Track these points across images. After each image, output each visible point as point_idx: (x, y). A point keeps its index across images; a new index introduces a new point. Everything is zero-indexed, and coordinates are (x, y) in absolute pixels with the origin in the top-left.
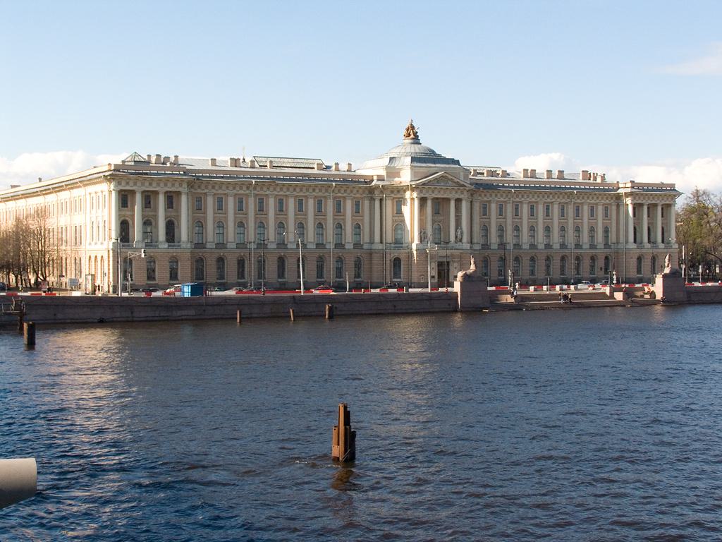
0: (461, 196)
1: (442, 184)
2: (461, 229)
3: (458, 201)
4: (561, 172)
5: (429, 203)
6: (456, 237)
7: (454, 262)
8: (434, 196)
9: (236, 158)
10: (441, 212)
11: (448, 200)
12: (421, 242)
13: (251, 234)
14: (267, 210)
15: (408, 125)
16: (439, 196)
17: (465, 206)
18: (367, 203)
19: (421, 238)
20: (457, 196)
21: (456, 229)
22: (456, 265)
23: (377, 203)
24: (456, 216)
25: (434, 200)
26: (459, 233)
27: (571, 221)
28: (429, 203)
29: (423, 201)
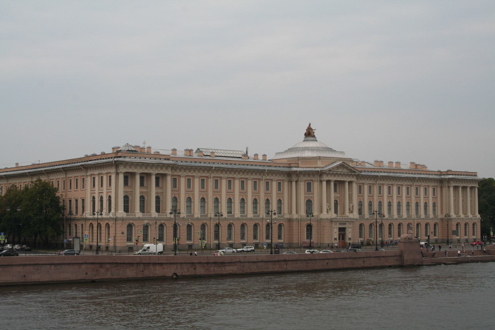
1: (340, 170)
3: (350, 183)
9: (190, 149)
12: (327, 212)
18: (286, 184)
22: (350, 230)
23: (294, 184)
28: (332, 184)
29: (328, 182)
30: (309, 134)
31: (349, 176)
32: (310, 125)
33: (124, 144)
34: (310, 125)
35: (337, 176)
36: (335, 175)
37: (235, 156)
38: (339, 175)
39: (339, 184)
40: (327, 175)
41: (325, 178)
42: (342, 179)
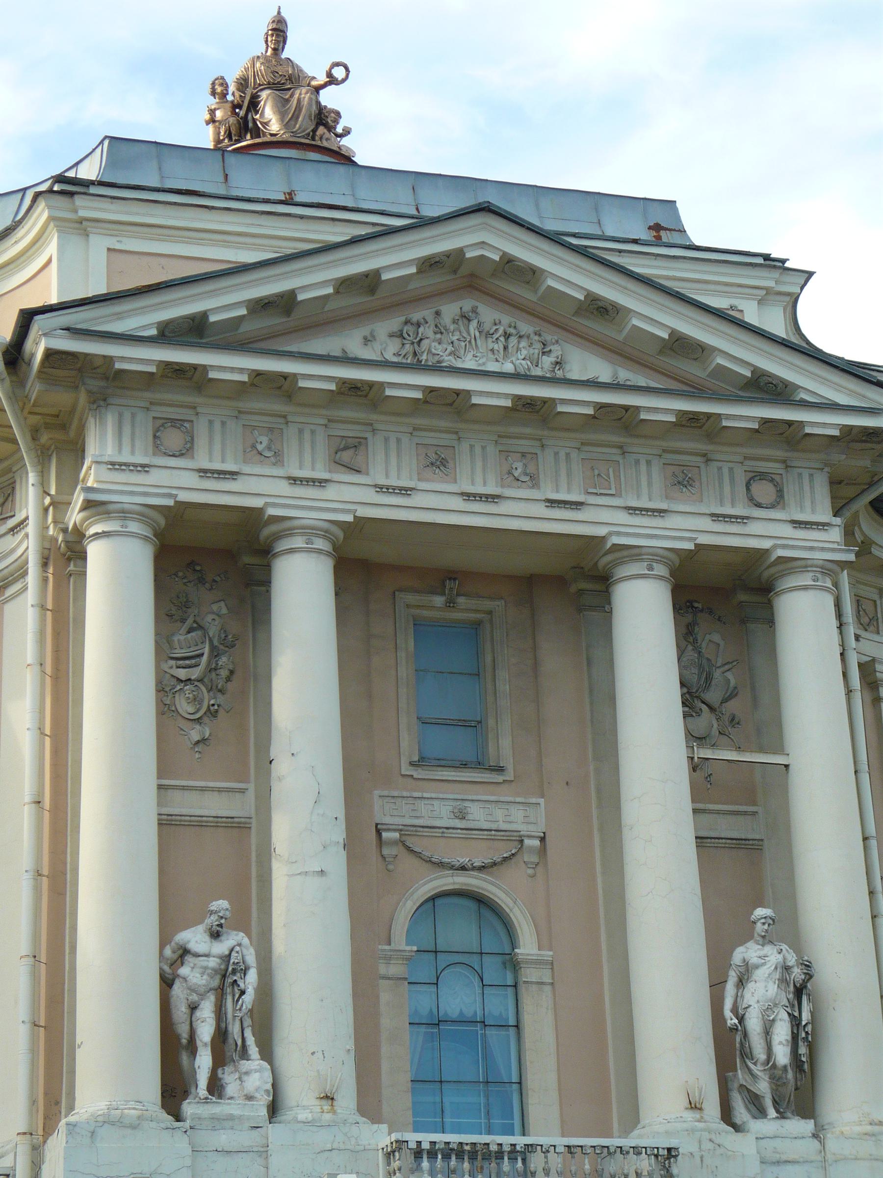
0: (765, 532)
2: (787, 929)
3: (725, 602)
5: (302, 593)
6: (730, 1046)
8: (351, 497)
10: (504, 746)
11: (578, 582)
12: (174, 1092)
15: (238, 53)
19: (174, 1047)
20: (690, 525)
21: (723, 935)
24: (707, 784)
25: (364, 566)
26: (762, 992)
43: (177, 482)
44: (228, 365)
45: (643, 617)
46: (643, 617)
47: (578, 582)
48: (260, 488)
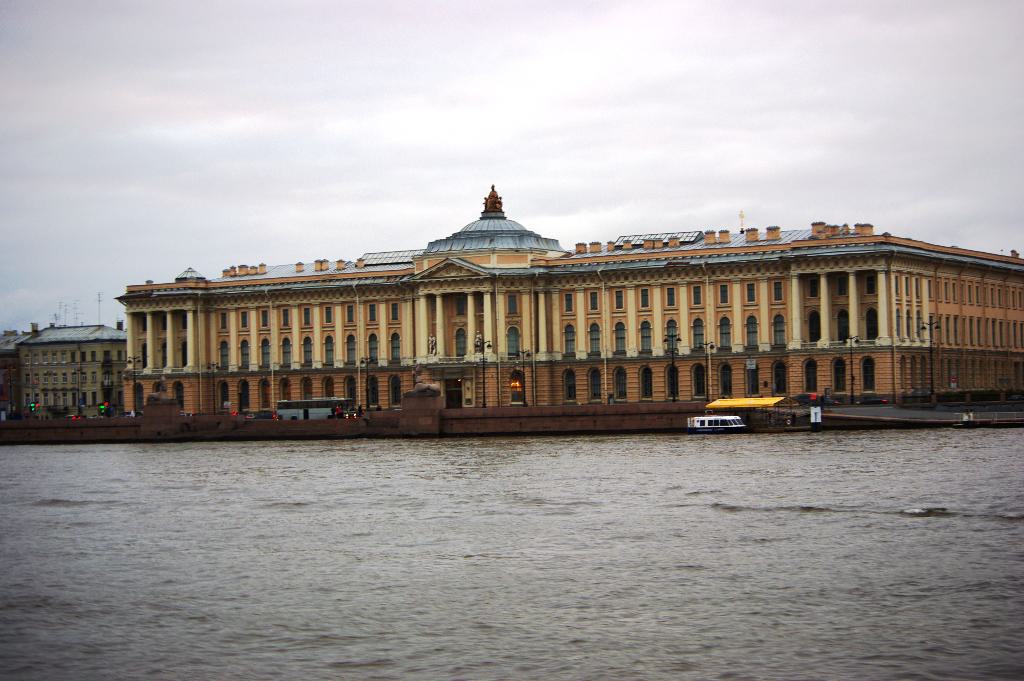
0: (481, 289)
1: (453, 275)
3: (479, 296)
4: (772, 230)
5: (439, 301)
7: (467, 379)
11: (464, 296)
13: (361, 351)
14: (521, 313)
16: (830, 270)
17: (487, 299)
20: (473, 289)
22: (468, 384)
25: (445, 296)
27: (710, 310)
28: (439, 301)
30: (493, 206)
31: (472, 282)
32: (493, 187)
33: (186, 269)
34: (493, 187)
35: (445, 287)
36: (441, 284)
37: (380, 262)
38: (449, 283)
39: (455, 302)
40: (426, 285)
41: (422, 291)
42: (457, 290)
43: (426, 292)
44: (426, 281)
45: (470, 301)
46: (470, 301)
47: (464, 296)
48: (434, 291)
